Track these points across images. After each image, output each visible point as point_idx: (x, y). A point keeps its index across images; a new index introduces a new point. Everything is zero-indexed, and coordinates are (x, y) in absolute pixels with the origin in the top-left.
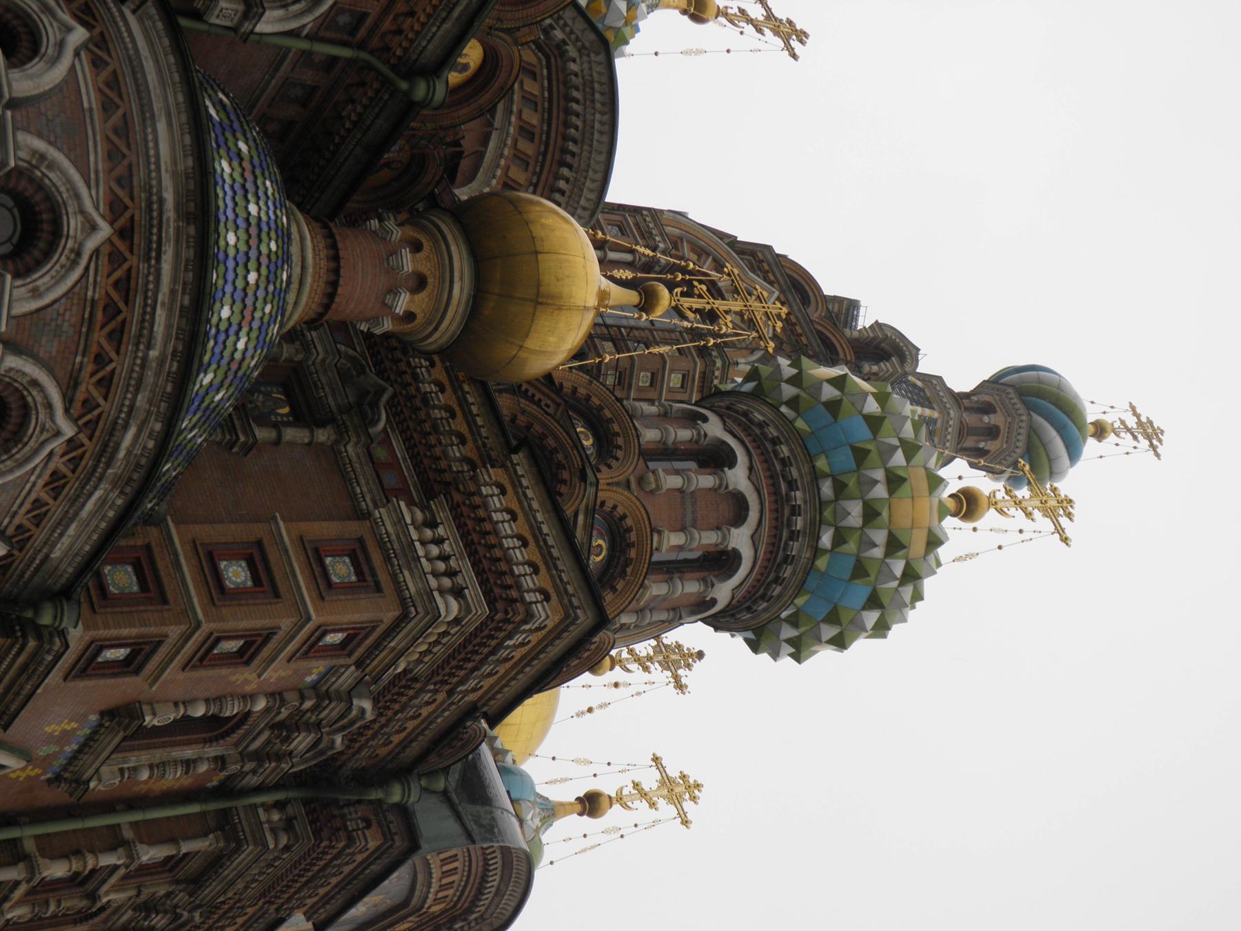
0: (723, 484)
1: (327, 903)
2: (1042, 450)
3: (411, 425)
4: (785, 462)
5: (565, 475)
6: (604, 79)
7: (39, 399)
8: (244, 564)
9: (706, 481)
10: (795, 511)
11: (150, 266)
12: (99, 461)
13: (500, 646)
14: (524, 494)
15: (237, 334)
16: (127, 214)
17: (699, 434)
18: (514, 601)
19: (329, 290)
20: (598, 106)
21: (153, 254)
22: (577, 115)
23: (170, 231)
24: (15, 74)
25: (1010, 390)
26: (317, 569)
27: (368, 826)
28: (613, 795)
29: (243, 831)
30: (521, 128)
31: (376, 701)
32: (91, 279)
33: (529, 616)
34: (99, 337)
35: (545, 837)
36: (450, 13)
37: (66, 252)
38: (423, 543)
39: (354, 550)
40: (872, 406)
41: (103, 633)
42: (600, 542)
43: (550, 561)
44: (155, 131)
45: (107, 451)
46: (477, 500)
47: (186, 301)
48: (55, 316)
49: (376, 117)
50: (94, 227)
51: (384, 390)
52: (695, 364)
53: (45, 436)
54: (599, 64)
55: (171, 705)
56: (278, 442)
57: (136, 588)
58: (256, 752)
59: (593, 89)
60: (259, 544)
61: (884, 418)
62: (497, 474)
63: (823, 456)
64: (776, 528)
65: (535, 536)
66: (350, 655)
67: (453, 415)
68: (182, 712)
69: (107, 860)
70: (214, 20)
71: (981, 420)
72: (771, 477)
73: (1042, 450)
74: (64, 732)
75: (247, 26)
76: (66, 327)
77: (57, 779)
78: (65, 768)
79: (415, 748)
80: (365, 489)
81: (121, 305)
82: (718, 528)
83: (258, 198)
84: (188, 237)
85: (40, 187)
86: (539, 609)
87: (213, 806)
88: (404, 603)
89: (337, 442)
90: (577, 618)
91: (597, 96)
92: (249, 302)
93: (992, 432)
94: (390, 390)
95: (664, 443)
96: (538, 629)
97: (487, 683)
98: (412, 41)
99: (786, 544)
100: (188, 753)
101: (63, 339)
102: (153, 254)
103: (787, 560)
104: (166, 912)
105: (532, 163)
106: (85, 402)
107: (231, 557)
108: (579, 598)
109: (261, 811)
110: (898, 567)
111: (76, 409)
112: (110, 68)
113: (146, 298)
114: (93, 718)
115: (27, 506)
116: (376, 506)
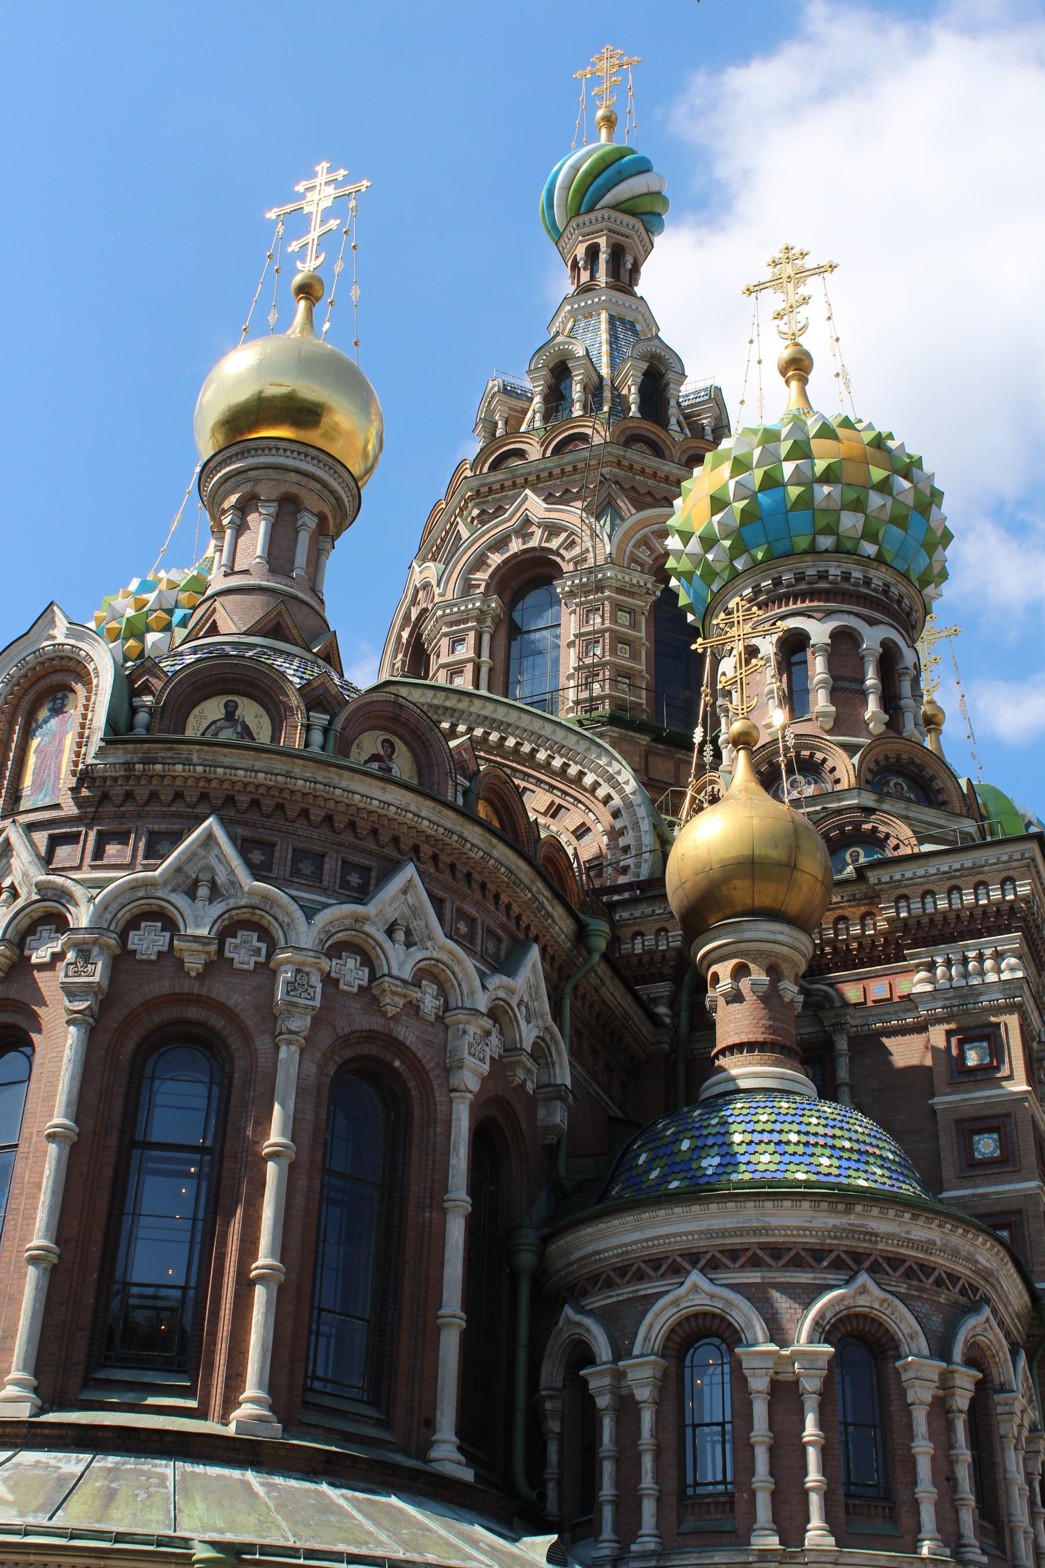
0: (823, 649)
2: (637, 200)
4: (800, 578)
8: (976, 1138)
10: (846, 577)
25: (574, 224)
33: (1026, 899)
42: (892, 784)
43: (975, 869)
46: (912, 923)
63: (795, 539)
65: (950, 878)
70: (565, 1126)
82: (863, 658)
91: (448, 704)
92: (863, 1148)
93: (617, 253)
103: (886, 590)
107: (968, 1148)
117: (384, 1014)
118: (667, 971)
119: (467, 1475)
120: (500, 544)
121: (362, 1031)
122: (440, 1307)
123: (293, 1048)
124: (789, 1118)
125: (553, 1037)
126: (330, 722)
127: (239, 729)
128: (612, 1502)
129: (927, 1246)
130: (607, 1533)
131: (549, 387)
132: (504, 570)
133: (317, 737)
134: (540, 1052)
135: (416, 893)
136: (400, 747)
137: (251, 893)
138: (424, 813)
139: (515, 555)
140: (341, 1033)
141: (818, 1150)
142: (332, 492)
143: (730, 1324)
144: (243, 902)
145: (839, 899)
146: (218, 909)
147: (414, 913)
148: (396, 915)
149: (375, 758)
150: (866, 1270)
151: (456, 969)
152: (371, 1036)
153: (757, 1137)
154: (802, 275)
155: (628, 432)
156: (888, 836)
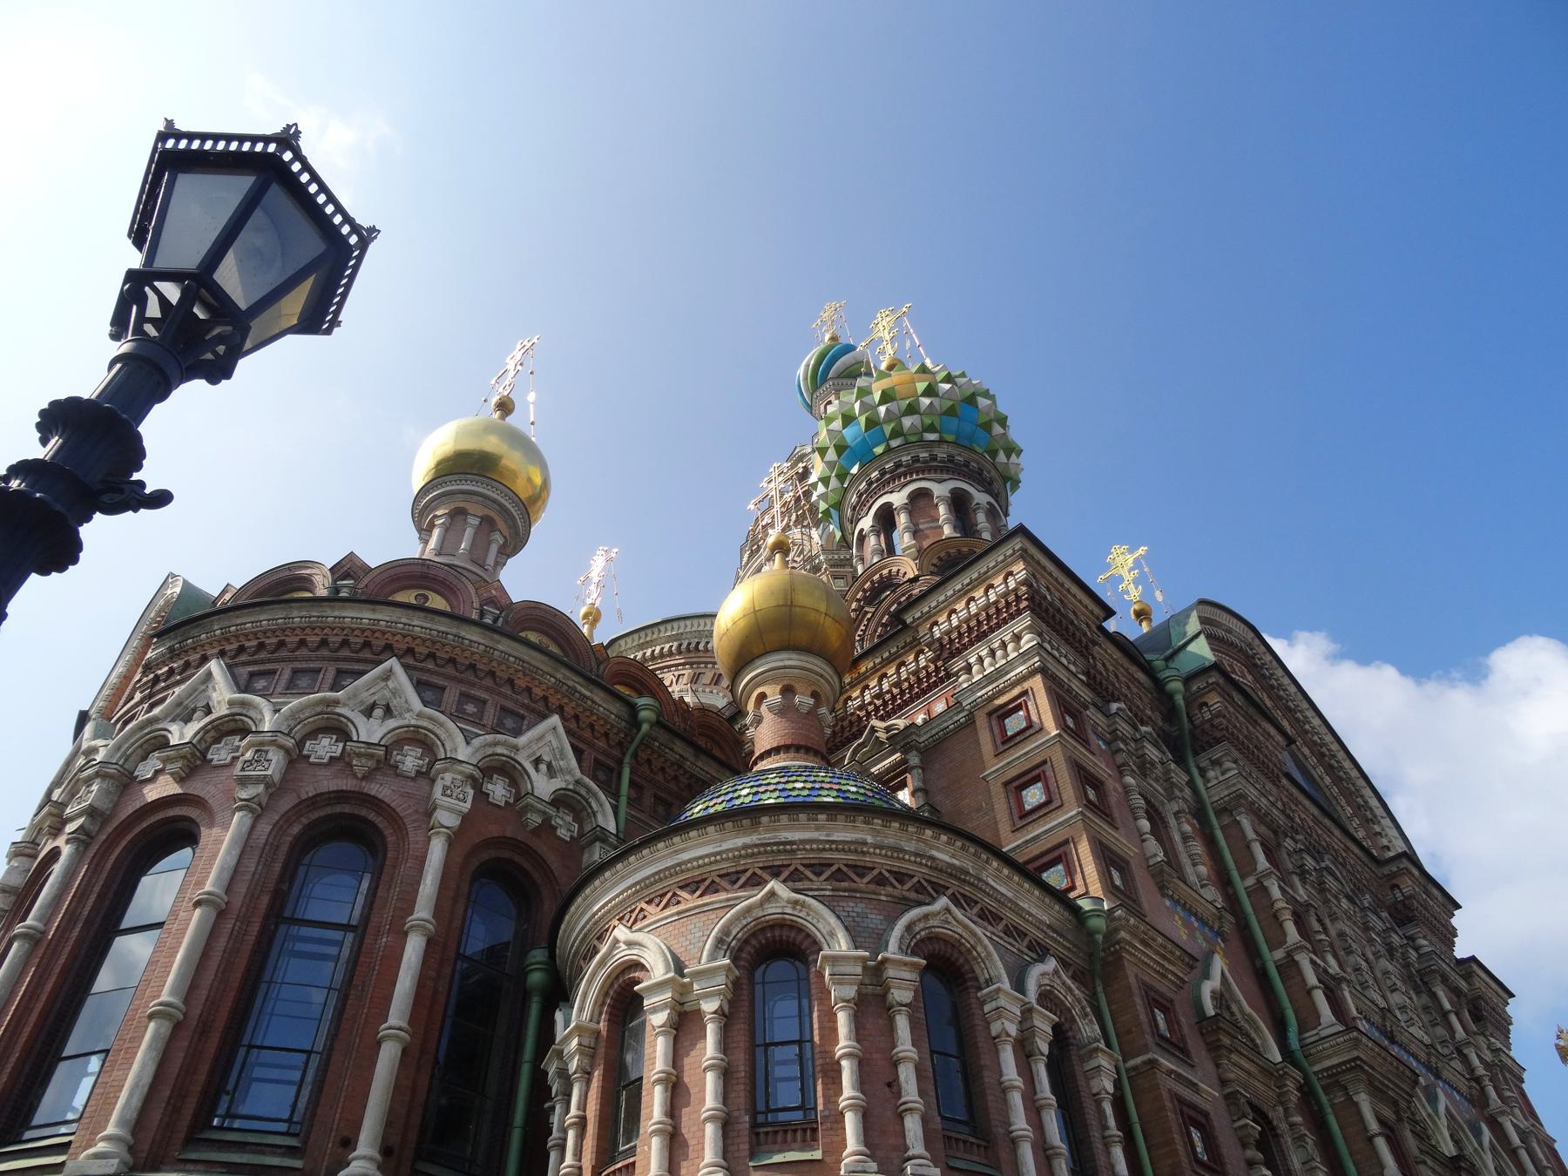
0: (905, 507)
1: (1269, 734)
4: (883, 473)
6: (636, 636)
7: (922, 925)
8: (1024, 793)
9: (902, 519)
10: (916, 459)
11: (798, 850)
12: (964, 881)
13: (1051, 604)
15: (845, 792)
19: (802, 751)
20: (655, 637)
21: (788, 847)
26: (1019, 738)
27: (1206, 704)
29: (1229, 795)
31: (1109, 702)
32: (816, 893)
34: (862, 883)
36: (587, 698)
37: (796, 913)
40: (837, 425)
44: (690, 861)
45: (957, 874)
48: (850, 919)
49: (671, 750)
50: (772, 894)
53: (950, 919)
54: (626, 643)
55: (1144, 844)
58: (1165, 790)
59: (643, 644)
60: (1006, 784)
65: (965, 593)
66: (1081, 713)
69: (1276, 892)
74: (1183, 924)
75: (613, 840)
77: (1220, 934)
78: (1211, 928)
79: (1141, 676)
80: (950, 722)
83: (736, 790)
84: (771, 821)
85: (746, 942)
89: (918, 750)
90: (1021, 549)
91: (648, 639)
100: (1177, 837)
101: (868, 911)
102: (788, 847)
103: (951, 459)
106: (917, 892)
107: (1020, 802)
108: (1007, 550)
109: (1209, 785)
113: (824, 849)
117: (355, 776)
121: (329, 793)
125: (589, 790)
129: (857, 847)
134: (560, 800)
138: (415, 623)
140: (304, 796)
142: (494, 501)
147: (394, 694)
148: (376, 697)
152: (341, 796)
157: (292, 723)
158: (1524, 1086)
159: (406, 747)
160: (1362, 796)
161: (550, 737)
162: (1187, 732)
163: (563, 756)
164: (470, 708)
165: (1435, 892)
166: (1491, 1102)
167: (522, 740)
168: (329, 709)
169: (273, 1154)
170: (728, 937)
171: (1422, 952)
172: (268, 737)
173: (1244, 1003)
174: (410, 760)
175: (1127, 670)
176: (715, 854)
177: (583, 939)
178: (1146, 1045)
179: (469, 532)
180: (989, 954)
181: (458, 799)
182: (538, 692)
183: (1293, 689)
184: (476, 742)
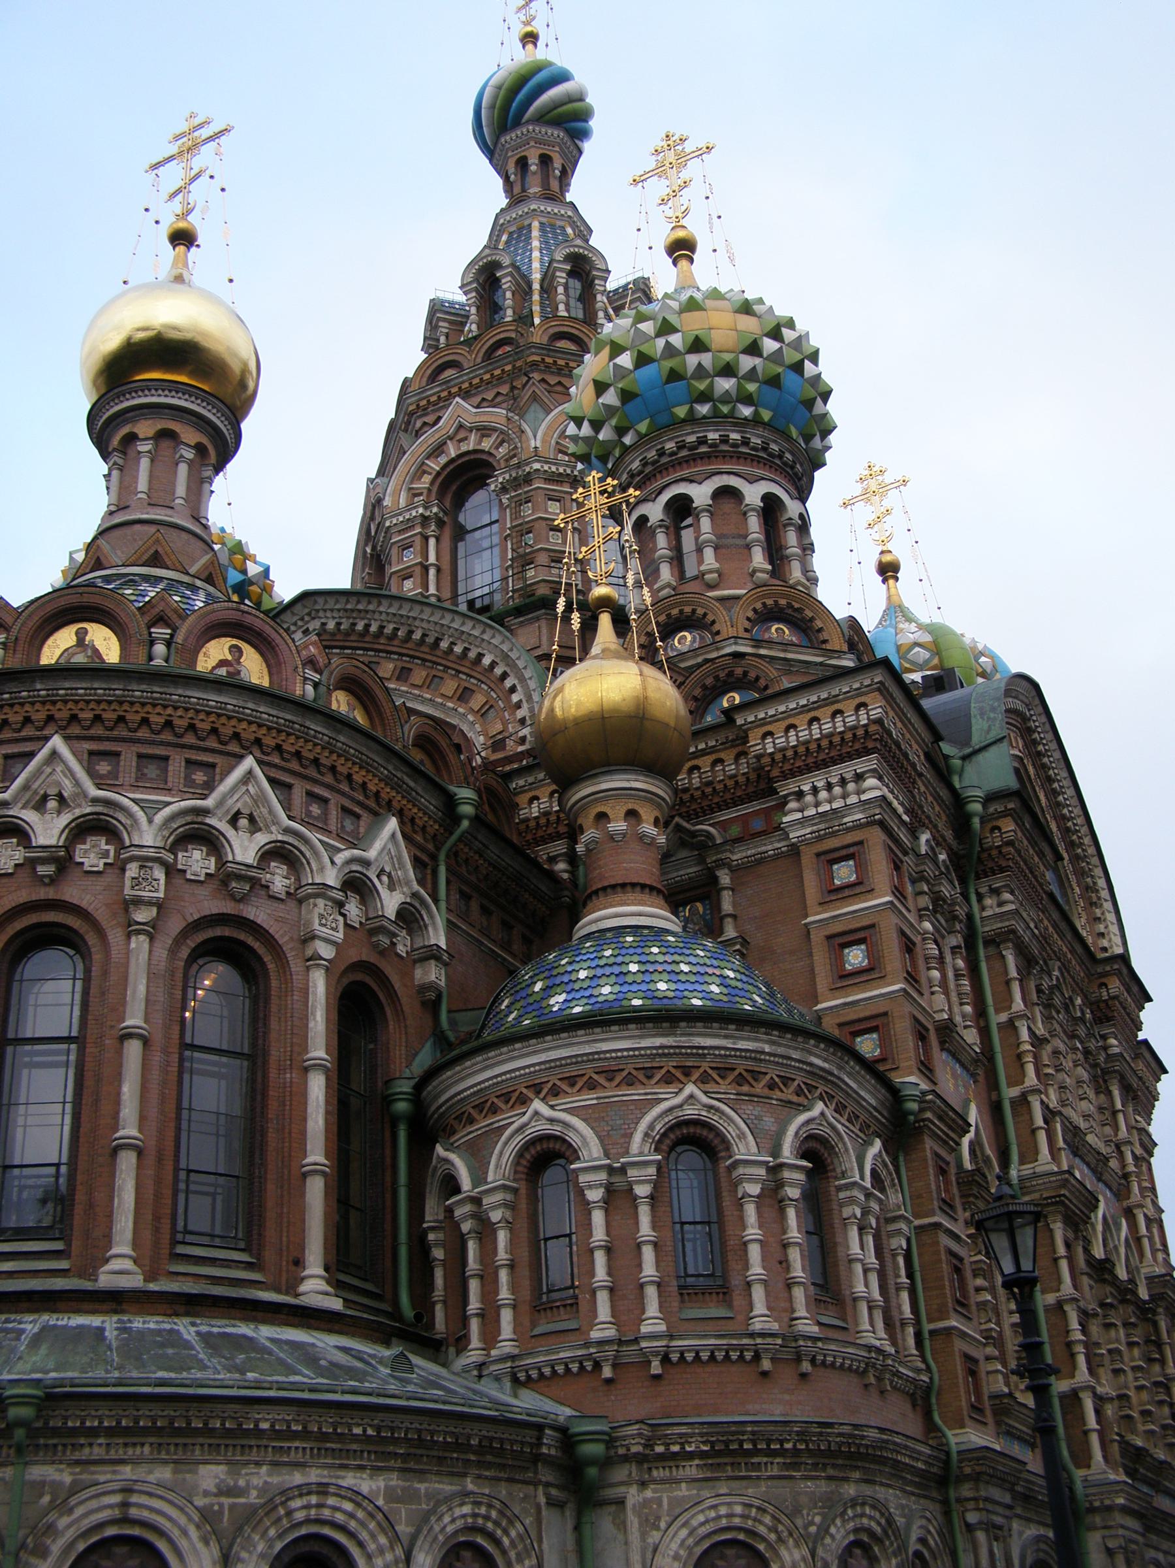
2: (560, 110)
3: (705, 803)
5: (739, 671)
6: (343, 599)
7: (804, 1129)
8: (846, 951)
9: (705, 523)
10: (725, 440)
14: (771, 716)
16: (673, 1071)
17: (660, 526)
18: (866, 732)
19: (647, 890)
20: (371, 607)
21: (700, 1053)
22: (382, 627)
23: (683, 1041)
24: (583, 1154)
26: (847, 892)
27: (999, 829)
28: (880, 549)
30: (398, 679)
33: (879, 722)
34: (759, 1088)
35: (925, 619)
36: (412, 789)
38: (817, 805)
39: (828, 861)
40: (625, 360)
41: (912, 1063)
46: (778, 757)
47: (733, 1027)
50: (691, 1096)
51: (677, 825)
52: (539, 488)
56: (734, 917)
57: (875, 1036)
58: (946, 921)
59: (352, 610)
60: (829, 937)
61: (639, 351)
62: (754, 739)
64: (740, 457)
65: (809, 710)
66: (902, 862)
67: (697, 768)
68: (937, 989)
69: (1024, 1035)
70: (443, 983)
71: (535, 173)
72: (694, 460)
73: (560, 110)
75: (445, 957)
76: (756, 1113)
77: (973, 1075)
78: (968, 1070)
80: (770, 847)
81: (736, 1073)
82: (745, 514)
86: (876, 713)
87: (982, 953)
88: (870, 823)
89: (730, 868)
91: (360, 607)
92: (702, 970)
93: (545, 160)
94: (677, 819)
95: (672, 559)
96: (886, 713)
97: (915, 746)
98: (430, 817)
99: (753, 449)
104: (1041, 978)
105: (434, 672)
106: (798, 1095)
107: (840, 960)
109: (985, 914)
110: (770, 345)
111: (801, 1100)
112: (559, 1083)
114: (944, 1055)
115: (852, 1127)
116: (787, 838)
118: (562, 829)
119: (336, 1304)
120: (438, 450)
122: (305, 1156)
123: (142, 937)
124: (631, 951)
126: (172, 636)
127: (89, 653)
128: (477, 1315)
129: (755, 1056)
130: (475, 1342)
131: (481, 297)
132: (443, 476)
133: (160, 649)
134: (408, 917)
135: (257, 783)
136: (247, 649)
137: (95, 801)
139: (452, 461)
140: (190, 920)
141: (655, 977)
143: (570, 1145)
144: (88, 810)
145: (714, 743)
146: (65, 819)
147: (255, 802)
148: (239, 805)
149: (222, 663)
150: (694, 1083)
151: (303, 849)
153: (599, 972)
154: (682, 161)
155: (552, 331)
156: (757, 678)
157: (166, 833)
158: (1152, 1160)
159: (273, 864)
160: (1092, 877)
161: (390, 846)
162: (975, 856)
163: (402, 866)
164: (315, 810)
165: (1135, 989)
166: (1132, 1196)
167: (372, 854)
168: (200, 819)
169: (237, 1268)
170: (652, 1130)
171: (1110, 1052)
172: (151, 853)
173: (987, 1146)
174: (279, 879)
175: (934, 789)
176: (634, 1049)
177: (478, 1091)
178: (933, 1210)
179: (183, 469)
180: (847, 1150)
181: (332, 929)
182: (372, 787)
183: (1057, 755)
184: (340, 858)
